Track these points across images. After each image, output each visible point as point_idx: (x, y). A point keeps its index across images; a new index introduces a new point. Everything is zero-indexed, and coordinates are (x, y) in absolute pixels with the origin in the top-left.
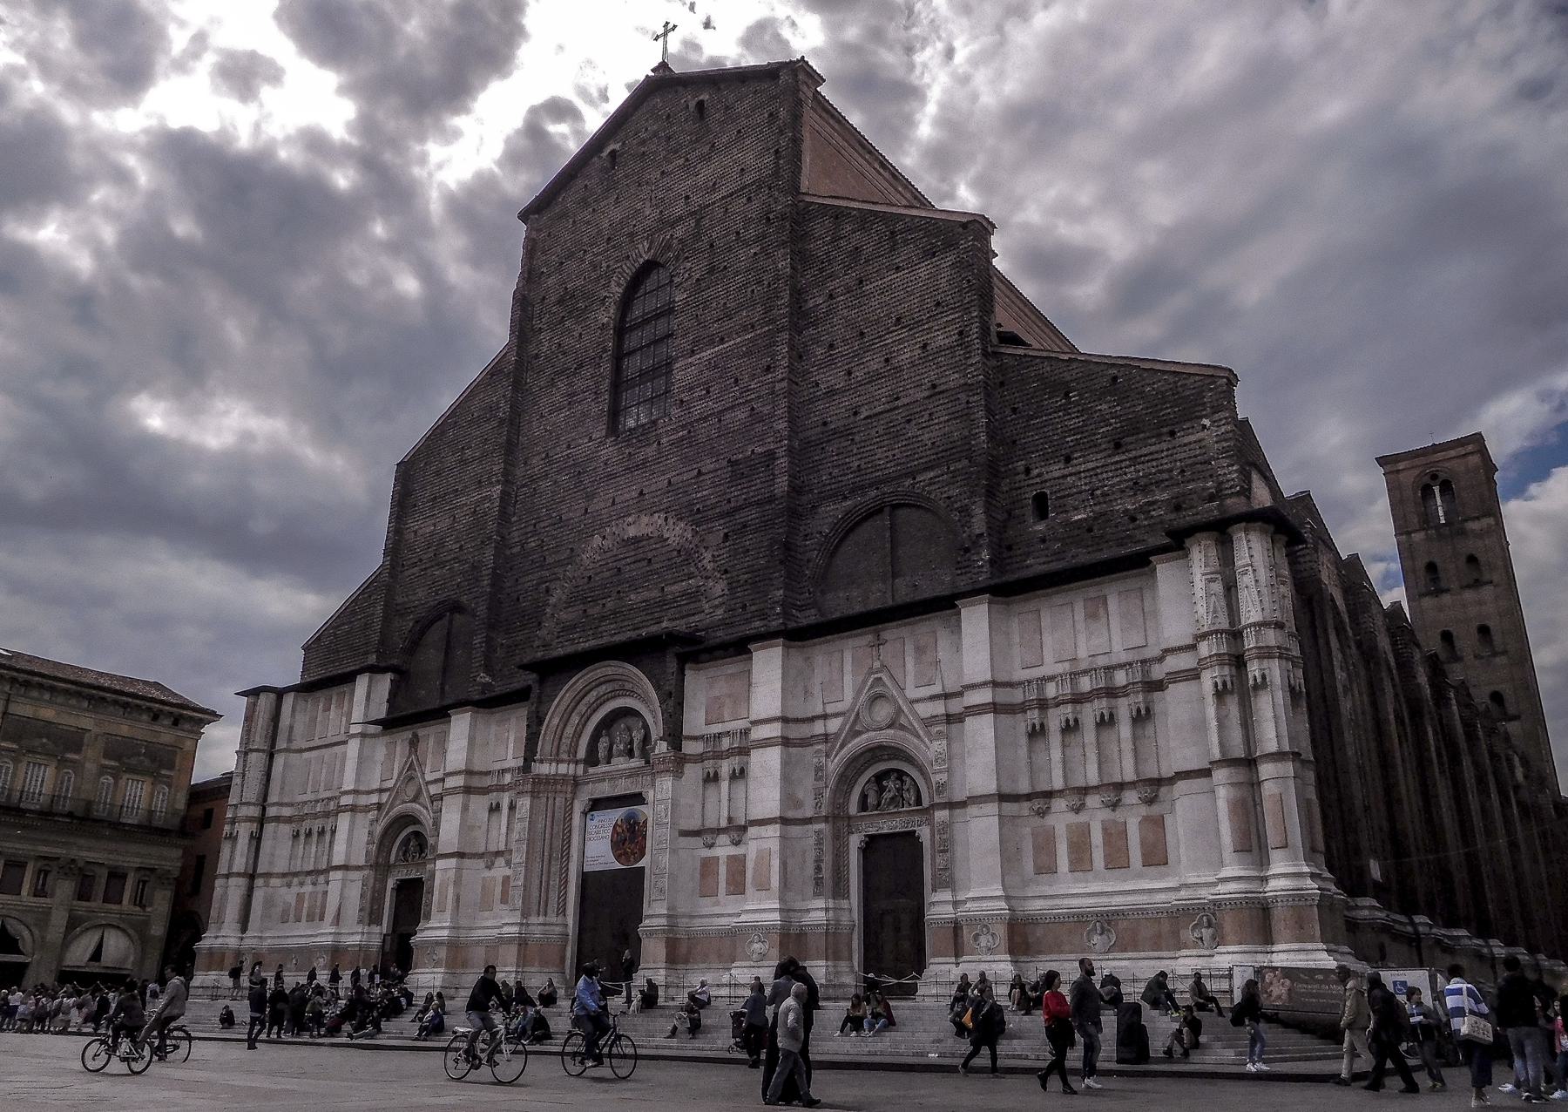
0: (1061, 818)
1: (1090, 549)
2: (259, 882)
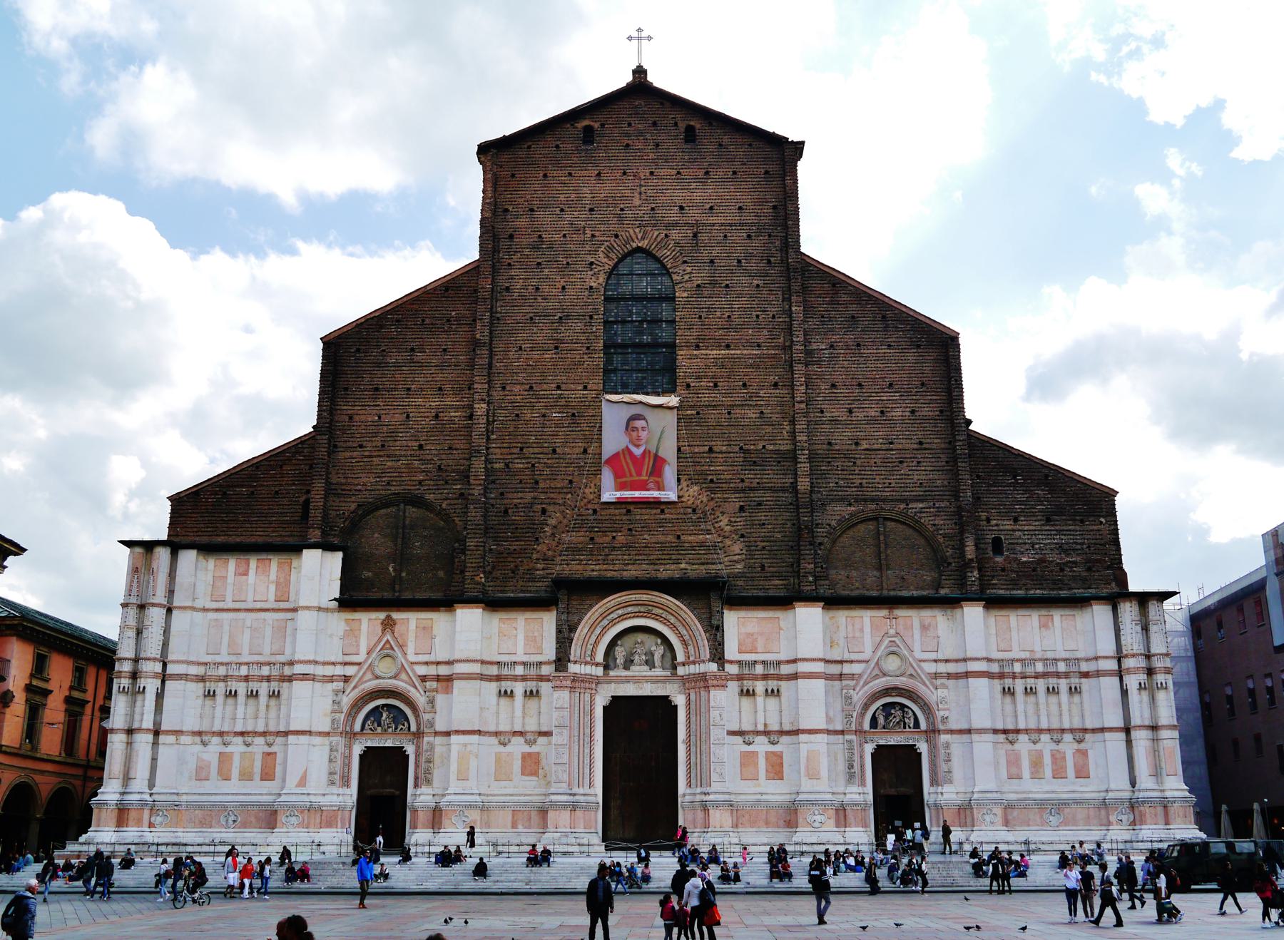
2: (162, 738)
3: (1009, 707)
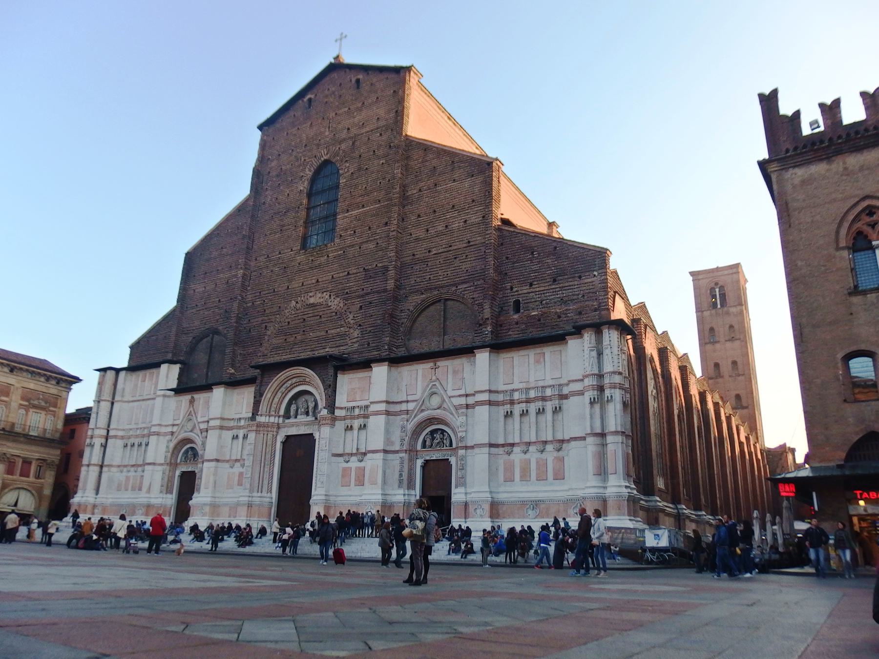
0: (517, 455)
1: (539, 329)
2: (105, 469)
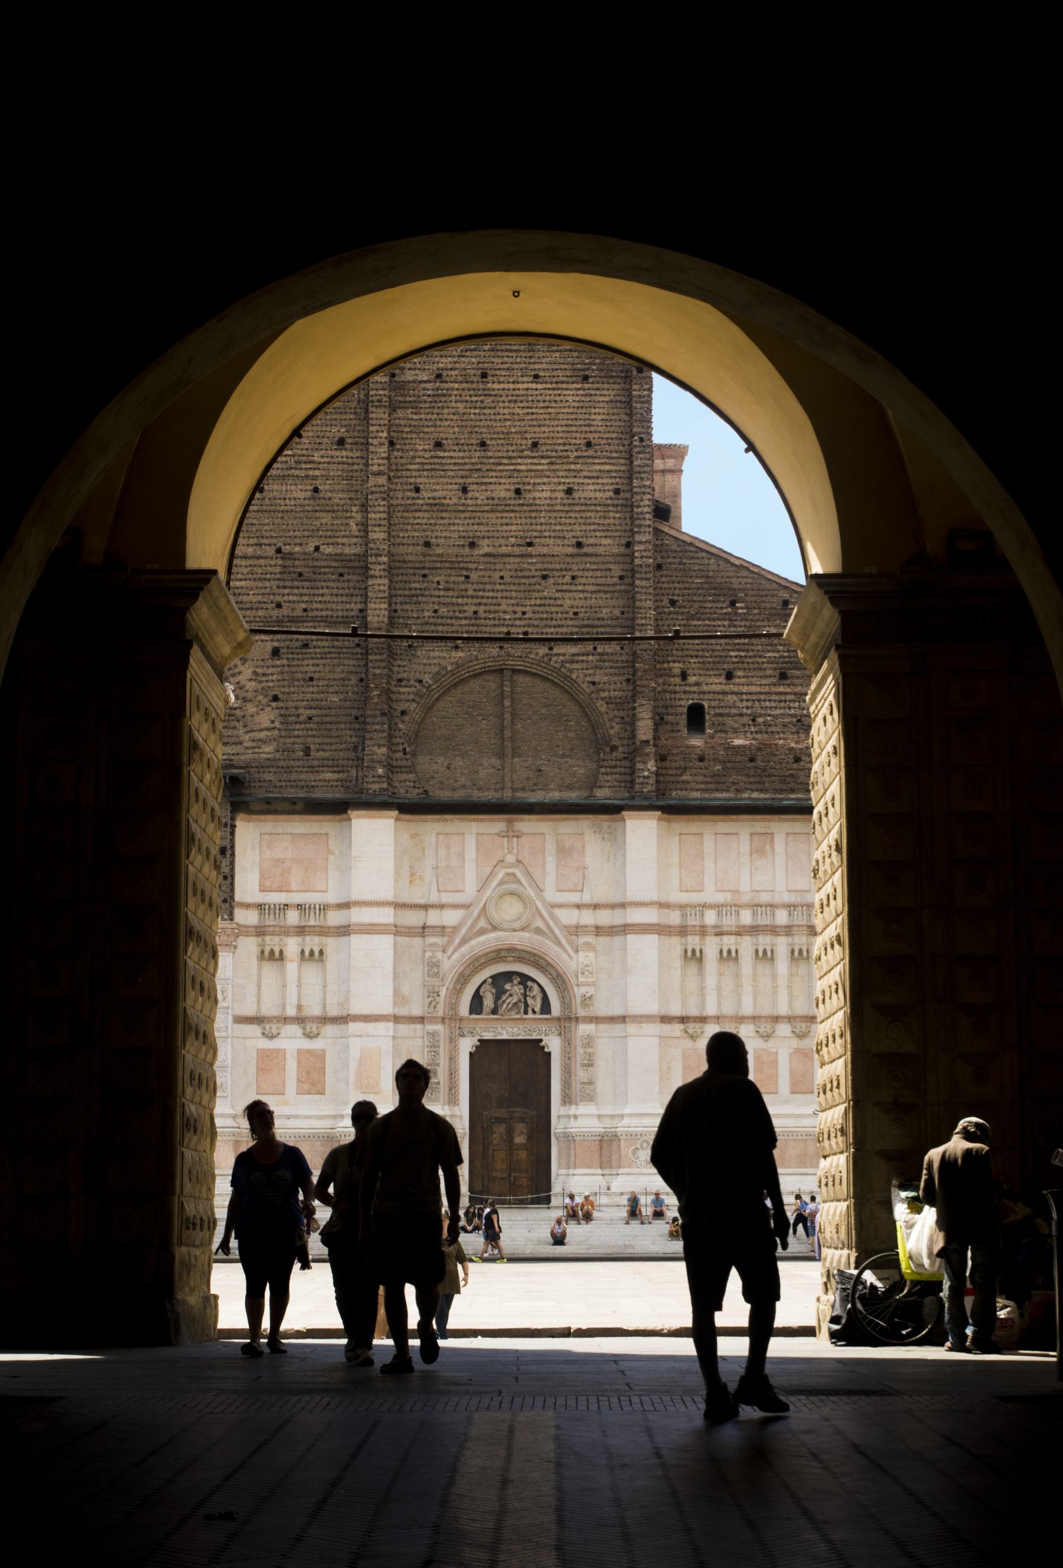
1: (752, 779)
3: (692, 982)
